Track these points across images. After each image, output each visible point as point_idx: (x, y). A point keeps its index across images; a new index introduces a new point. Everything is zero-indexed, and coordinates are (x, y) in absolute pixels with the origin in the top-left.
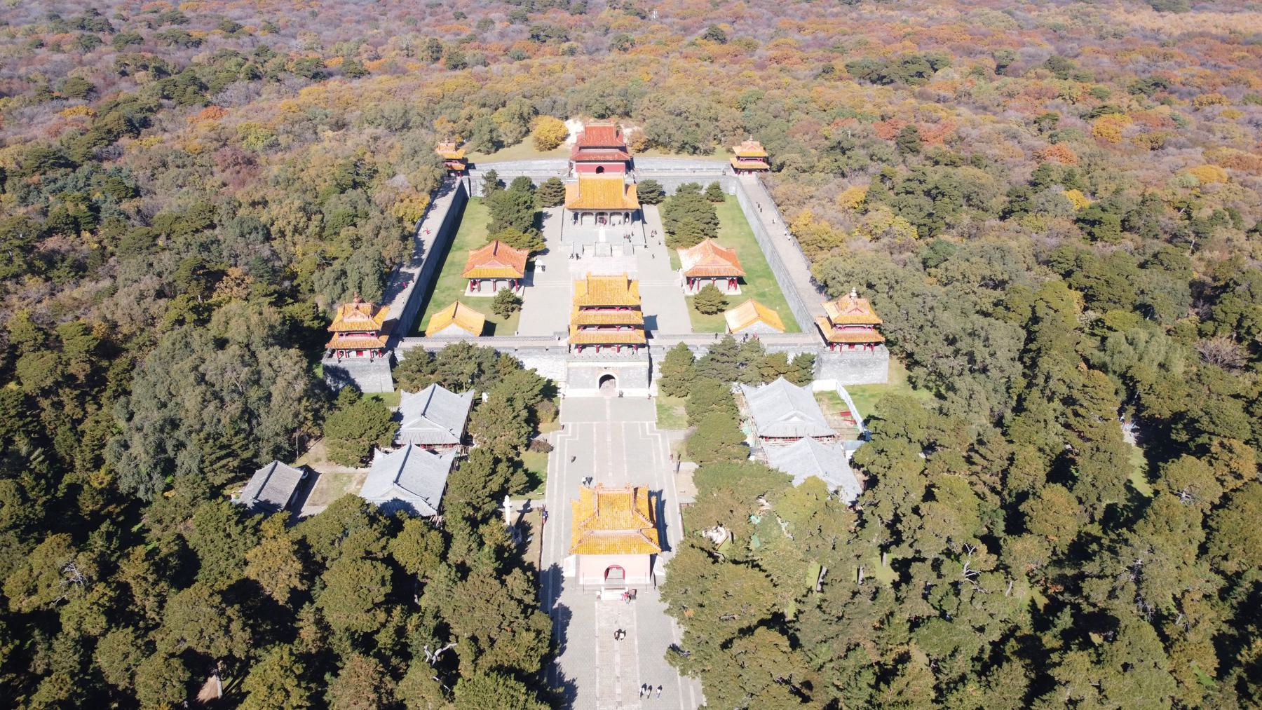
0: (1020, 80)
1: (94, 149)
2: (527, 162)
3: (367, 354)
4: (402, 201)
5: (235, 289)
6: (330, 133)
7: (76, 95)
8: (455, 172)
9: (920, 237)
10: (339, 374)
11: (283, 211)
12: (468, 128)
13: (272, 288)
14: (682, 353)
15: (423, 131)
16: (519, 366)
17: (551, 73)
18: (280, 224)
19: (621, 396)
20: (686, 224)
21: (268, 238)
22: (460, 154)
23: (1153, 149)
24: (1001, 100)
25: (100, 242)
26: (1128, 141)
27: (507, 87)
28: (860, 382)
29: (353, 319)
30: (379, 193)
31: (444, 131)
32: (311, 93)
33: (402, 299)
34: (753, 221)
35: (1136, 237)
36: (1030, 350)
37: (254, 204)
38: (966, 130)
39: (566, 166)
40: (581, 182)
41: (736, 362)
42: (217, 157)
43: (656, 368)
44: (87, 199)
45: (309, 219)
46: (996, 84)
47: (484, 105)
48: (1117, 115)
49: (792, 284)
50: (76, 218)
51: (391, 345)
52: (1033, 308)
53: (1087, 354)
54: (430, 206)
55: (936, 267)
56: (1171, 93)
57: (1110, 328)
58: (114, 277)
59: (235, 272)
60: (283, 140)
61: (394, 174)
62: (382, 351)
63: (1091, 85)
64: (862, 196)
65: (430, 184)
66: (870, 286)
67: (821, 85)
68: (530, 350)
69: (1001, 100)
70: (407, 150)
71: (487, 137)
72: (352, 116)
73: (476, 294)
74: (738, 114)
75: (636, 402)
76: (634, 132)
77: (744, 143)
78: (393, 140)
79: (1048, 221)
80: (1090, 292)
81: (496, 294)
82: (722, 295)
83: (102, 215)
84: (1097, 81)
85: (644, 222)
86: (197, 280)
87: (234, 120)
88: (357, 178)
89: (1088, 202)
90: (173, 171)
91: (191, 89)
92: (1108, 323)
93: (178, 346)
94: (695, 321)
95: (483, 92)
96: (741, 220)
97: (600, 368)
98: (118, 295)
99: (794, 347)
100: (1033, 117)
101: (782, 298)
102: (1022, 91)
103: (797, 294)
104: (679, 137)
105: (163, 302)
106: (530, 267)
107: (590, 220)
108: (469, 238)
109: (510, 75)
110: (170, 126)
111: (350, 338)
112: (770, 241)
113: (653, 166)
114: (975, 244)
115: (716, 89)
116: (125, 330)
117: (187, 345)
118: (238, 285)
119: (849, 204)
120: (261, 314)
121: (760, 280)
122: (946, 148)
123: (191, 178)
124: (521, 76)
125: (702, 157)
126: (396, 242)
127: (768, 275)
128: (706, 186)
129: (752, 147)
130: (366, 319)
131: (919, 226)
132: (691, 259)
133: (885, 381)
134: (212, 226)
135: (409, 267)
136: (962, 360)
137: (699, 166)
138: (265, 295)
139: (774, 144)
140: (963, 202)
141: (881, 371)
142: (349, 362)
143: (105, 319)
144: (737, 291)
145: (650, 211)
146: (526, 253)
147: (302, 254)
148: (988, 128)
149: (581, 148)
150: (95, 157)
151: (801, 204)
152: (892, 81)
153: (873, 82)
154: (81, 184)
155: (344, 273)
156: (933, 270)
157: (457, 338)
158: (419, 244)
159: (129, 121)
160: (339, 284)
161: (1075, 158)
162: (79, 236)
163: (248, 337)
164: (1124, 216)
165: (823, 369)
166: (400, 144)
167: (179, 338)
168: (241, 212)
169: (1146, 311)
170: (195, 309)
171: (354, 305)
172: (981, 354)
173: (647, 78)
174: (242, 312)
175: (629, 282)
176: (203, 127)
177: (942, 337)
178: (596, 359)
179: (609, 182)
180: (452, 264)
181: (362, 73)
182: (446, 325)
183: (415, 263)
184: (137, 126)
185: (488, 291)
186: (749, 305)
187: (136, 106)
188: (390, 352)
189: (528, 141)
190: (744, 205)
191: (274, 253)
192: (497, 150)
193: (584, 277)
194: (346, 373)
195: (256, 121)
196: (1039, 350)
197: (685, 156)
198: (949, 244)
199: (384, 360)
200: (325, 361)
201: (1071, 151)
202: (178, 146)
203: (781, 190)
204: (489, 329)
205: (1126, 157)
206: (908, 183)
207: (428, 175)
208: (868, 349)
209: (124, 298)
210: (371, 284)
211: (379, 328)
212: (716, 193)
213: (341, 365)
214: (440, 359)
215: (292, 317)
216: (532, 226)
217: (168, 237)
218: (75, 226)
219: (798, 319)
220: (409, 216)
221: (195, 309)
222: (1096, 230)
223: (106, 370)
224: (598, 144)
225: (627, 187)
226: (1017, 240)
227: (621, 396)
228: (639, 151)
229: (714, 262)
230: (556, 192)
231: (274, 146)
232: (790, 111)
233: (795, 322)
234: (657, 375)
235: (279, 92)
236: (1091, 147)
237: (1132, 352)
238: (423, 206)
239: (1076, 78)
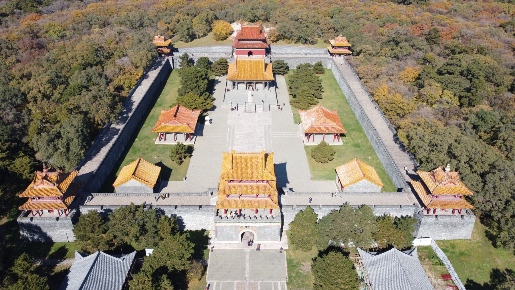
2: (208, 48)
8: (165, 54)
14: (306, 215)
18: (34, 92)
19: (258, 249)
20: (303, 91)
22: (167, 43)
28: (449, 238)
29: (41, 186)
30: (109, 70)
38: (464, 31)
39: (231, 51)
40: (238, 62)
49: (379, 142)
54: (144, 76)
60: (67, 33)
65: (144, 62)
70: (136, 41)
71: (186, 33)
73: (162, 142)
75: (271, 256)
76: (271, 30)
77: (337, 38)
85: (276, 87)
88: (100, 57)
94: (313, 169)
96: (336, 87)
97: (242, 227)
103: (386, 151)
104: (297, 33)
106: (201, 120)
107: (242, 86)
108: (167, 97)
112: (359, 104)
113: (283, 51)
119: (408, 79)
127: (359, 129)
129: (341, 41)
130: (52, 187)
131: (460, 97)
132: (309, 118)
133: (468, 238)
135: (118, 124)
137: (308, 51)
139: (354, 39)
144: (339, 143)
145: (281, 80)
148: (478, 30)
149: (239, 40)
155: (59, 136)
175: (266, 155)
179: (255, 62)
180: (153, 116)
182: (128, 180)
183: (123, 120)
189: (210, 34)
190: (337, 77)
192: (192, 40)
194: (39, 228)
197: (300, 45)
210: (75, 147)
212: (319, 68)
216: (206, 91)
219: (388, 170)
220: (127, 84)
224: (249, 38)
225: (266, 65)
227: (258, 249)
228: (274, 41)
229: (324, 123)
230: (223, 66)
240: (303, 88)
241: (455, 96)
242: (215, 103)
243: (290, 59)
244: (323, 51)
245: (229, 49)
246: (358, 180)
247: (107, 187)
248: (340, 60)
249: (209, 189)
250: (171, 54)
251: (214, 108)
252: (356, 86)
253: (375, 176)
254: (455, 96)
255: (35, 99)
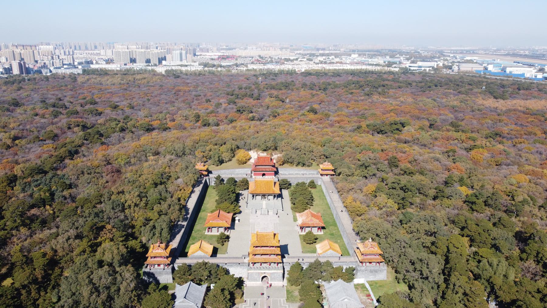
0: (439, 132)
1: (55, 165)
2: (233, 170)
3: (162, 266)
4: (180, 190)
5: (108, 234)
6: (152, 157)
7: (49, 138)
8: (203, 175)
9: (399, 209)
10: (151, 275)
11: (130, 198)
12: (209, 155)
13: (124, 233)
14: (297, 267)
15: (191, 156)
16: (227, 272)
17: (244, 130)
18: (129, 202)
20: (299, 201)
21: (123, 210)
22: (205, 168)
23: (497, 165)
24: (432, 141)
25: (53, 210)
26: (485, 162)
27: (227, 136)
29: (157, 251)
31: (199, 156)
32: (146, 139)
33: (178, 238)
34: (328, 198)
35: (491, 209)
36: (447, 268)
37: (119, 193)
39: (250, 172)
40: (256, 182)
41: (320, 271)
42: (105, 169)
43: (286, 273)
44: (50, 190)
45: (141, 200)
46: (430, 133)
47: (216, 145)
48: (481, 149)
50: (44, 199)
51: (173, 262)
52: (448, 247)
53: (472, 269)
54: (192, 192)
55: (406, 224)
56: (503, 138)
57: (481, 256)
58: (58, 227)
59: (109, 227)
60: (133, 160)
61: (178, 178)
62: (169, 265)
63: (469, 135)
64: (374, 189)
65: (192, 182)
66: (378, 235)
67: (356, 135)
68: (232, 264)
69: (432, 141)
70: (184, 166)
71: (217, 159)
72: (161, 150)
73: (210, 233)
74: (322, 149)
76: (278, 157)
78: (179, 160)
79: (453, 202)
80: (472, 238)
81: (218, 234)
82: (315, 236)
83: (55, 197)
84: (472, 132)
85: (282, 198)
86: (93, 231)
87: (113, 151)
88: (162, 180)
89: (470, 192)
90: (86, 176)
91: (97, 136)
92: (480, 254)
93: (82, 265)
94: (303, 247)
95: (216, 139)
96: (323, 197)
98: (58, 238)
99: (346, 263)
100: (445, 150)
101: (340, 236)
102: (440, 137)
105: (77, 241)
106: (233, 220)
107: (259, 198)
108: (208, 206)
109: (228, 130)
110: (86, 154)
111: (155, 259)
114: (422, 213)
115: (313, 137)
116: (60, 254)
117: (86, 264)
118: (109, 232)
119: (368, 192)
120: (118, 249)
121: (331, 227)
122: (409, 165)
123: (93, 179)
124: (232, 131)
125: (307, 168)
126: (177, 212)
127: (335, 225)
128: (309, 181)
130: (162, 251)
131: (398, 204)
132: (302, 218)
134: (101, 203)
135: (182, 222)
136: (417, 275)
137: (305, 172)
138: (121, 237)
139: (336, 164)
140: (417, 192)
141: (383, 274)
142: (155, 270)
143: (52, 249)
145: (285, 193)
146: (231, 214)
147: (138, 216)
148: (426, 156)
150: (54, 168)
151: (349, 191)
152: (386, 133)
153: (378, 133)
154: (47, 182)
155: (154, 227)
156: (405, 225)
157: (200, 257)
158: (187, 210)
159: (70, 152)
160: (152, 232)
161: (464, 170)
162: (45, 207)
163: (113, 260)
164: (486, 199)
165: (358, 274)
166: (181, 163)
167: (83, 261)
168: (113, 197)
169: (496, 247)
170: (91, 246)
171: (158, 245)
172: (426, 272)
173: (284, 132)
174: (110, 249)
175: (275, 235)
176: (100, 155)
177: (409, 261)
178: (260, 269)
180: (201, 218)
181: (167, 129)
182: (197, 251)
183: (185, 219)
184: (72, 154)
185: (215, 232)
186: (326, 242)
187: (73, 145)
188: (172, 265)
189: (234, 159)
190: (324, 191)
191: (125, 216)
192: (221, 164)
193: (255, 232)
195: (122, 152)
196: (451, 268)
197: (300, 167)
198: (411, 213)
199: (169, 269)
200: (144, 269)
201: (460, 168)
202: (89, 164)
203: (340, 185)
204: (215, 252)
205: (485, 170)
206: (393, 184)
207: (191, 178)
208: (378, 264)
209: (60, 239)
210: (165, 234)
211: (168, 255)
212: (313, 185)
213: (151, 271)
214: (193, 269)
215: (131, 247)
217: (82, 207)
218: (43, 203)
219: (348, 247)
221: (91, 246)
222: (474, 207)
223: (51, 275)
225: (275, 183)
226: (441, 212)
229: (311, 220)
230: (245, 184)
231: (129, 163)
232: (343, 147)
233: (346, 249)
234: (286, 276)
235: (132, 137)
236: (470, 165)
237: (491, 270)
238: (189, 192)
239: (463, 131)
240: (299, 199)
241: (395, 203)
242: (241, 209)
243: (292, 178)
244: (315, 172)
245: (248, 171)
246: (327, 251)
247: (185, 255)
248: (327, 179)
249: (243, 256)
250: (208, 175)
251: (240, 212)
252: (335, 197)
253: (338, 249)
254: (395, 203)
255: (130, 207)
